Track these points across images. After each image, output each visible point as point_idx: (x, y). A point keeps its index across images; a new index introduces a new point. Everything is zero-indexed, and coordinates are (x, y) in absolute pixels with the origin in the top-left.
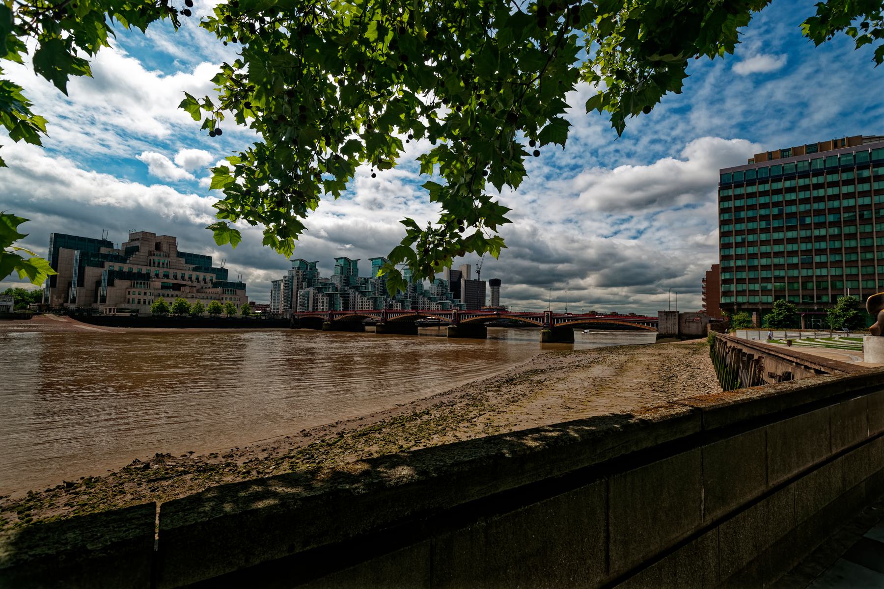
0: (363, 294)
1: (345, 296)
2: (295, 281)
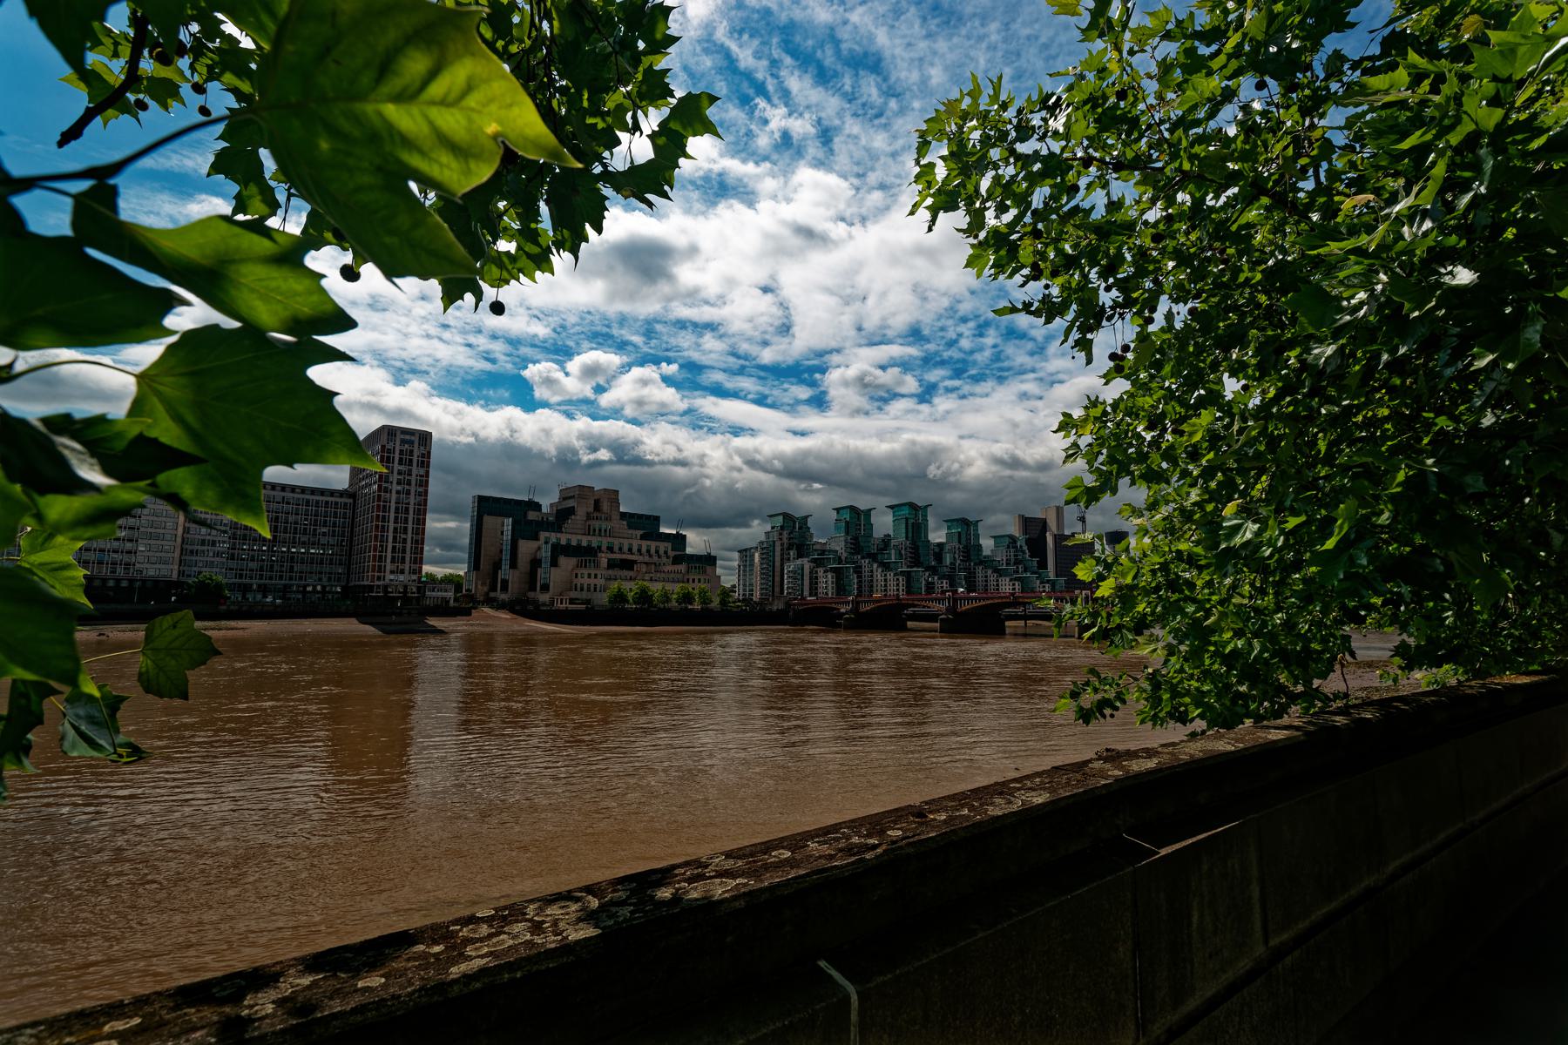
0: (886, 566)
2: (778, 548)
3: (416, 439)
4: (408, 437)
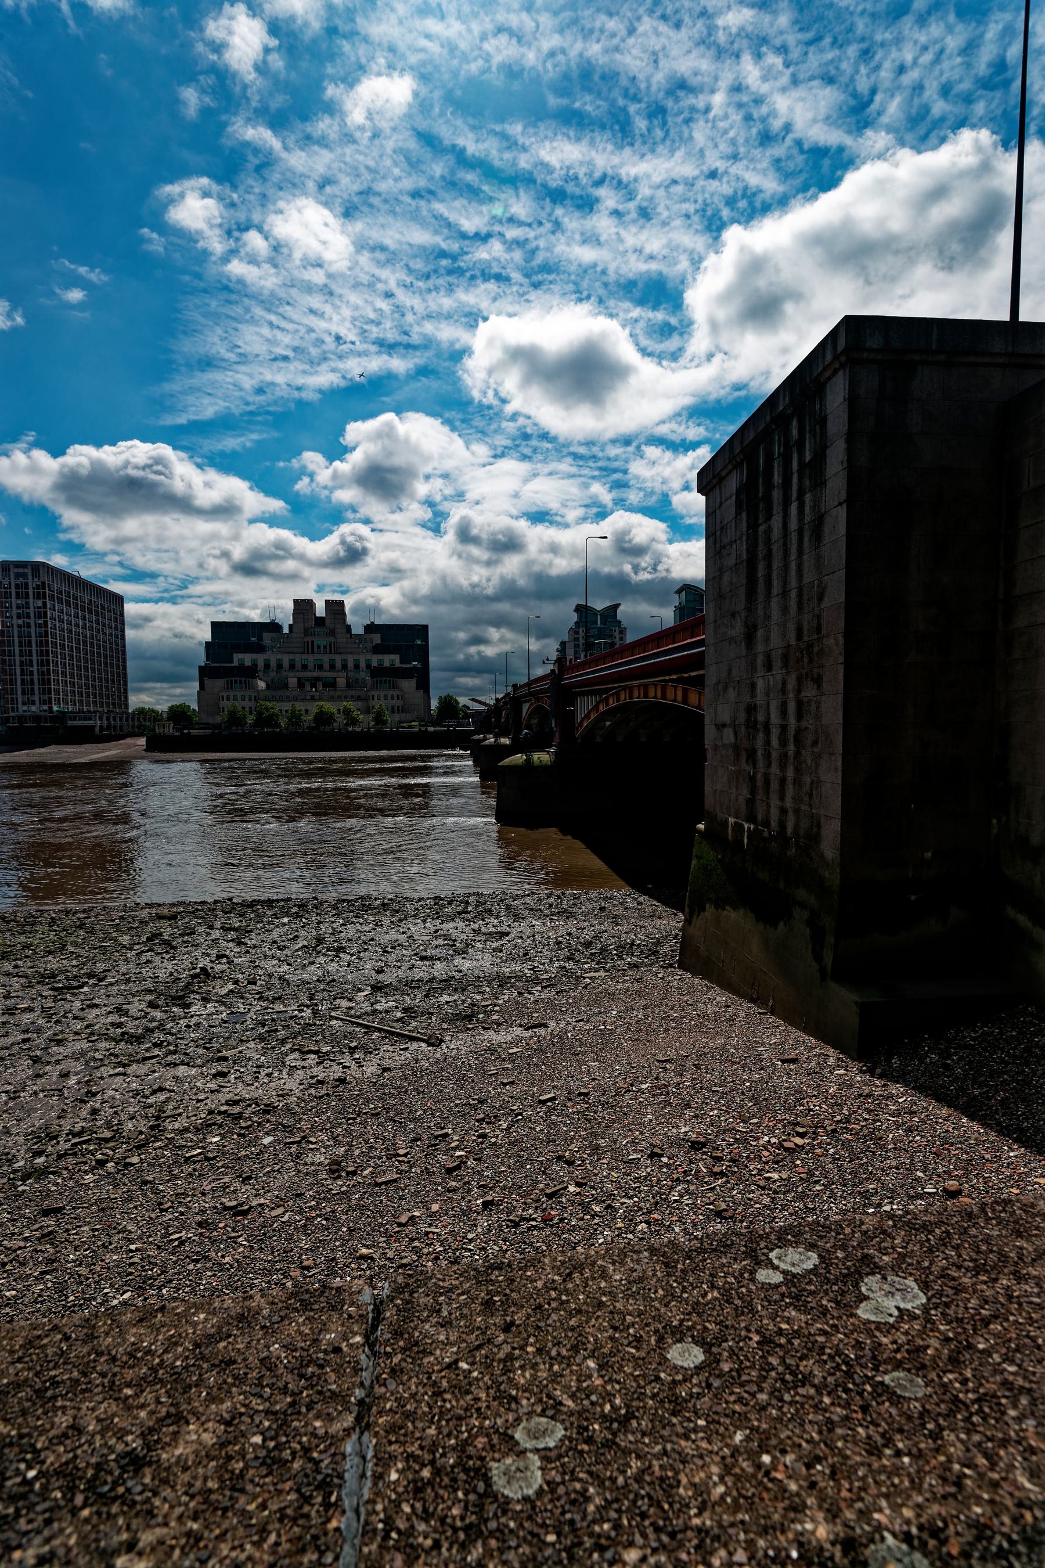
3: (28, 571)
4: (21, 570)
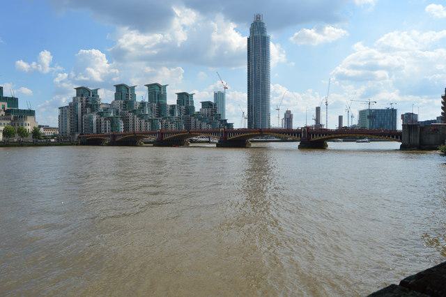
0: (141, 117)
1: (126, 120)
